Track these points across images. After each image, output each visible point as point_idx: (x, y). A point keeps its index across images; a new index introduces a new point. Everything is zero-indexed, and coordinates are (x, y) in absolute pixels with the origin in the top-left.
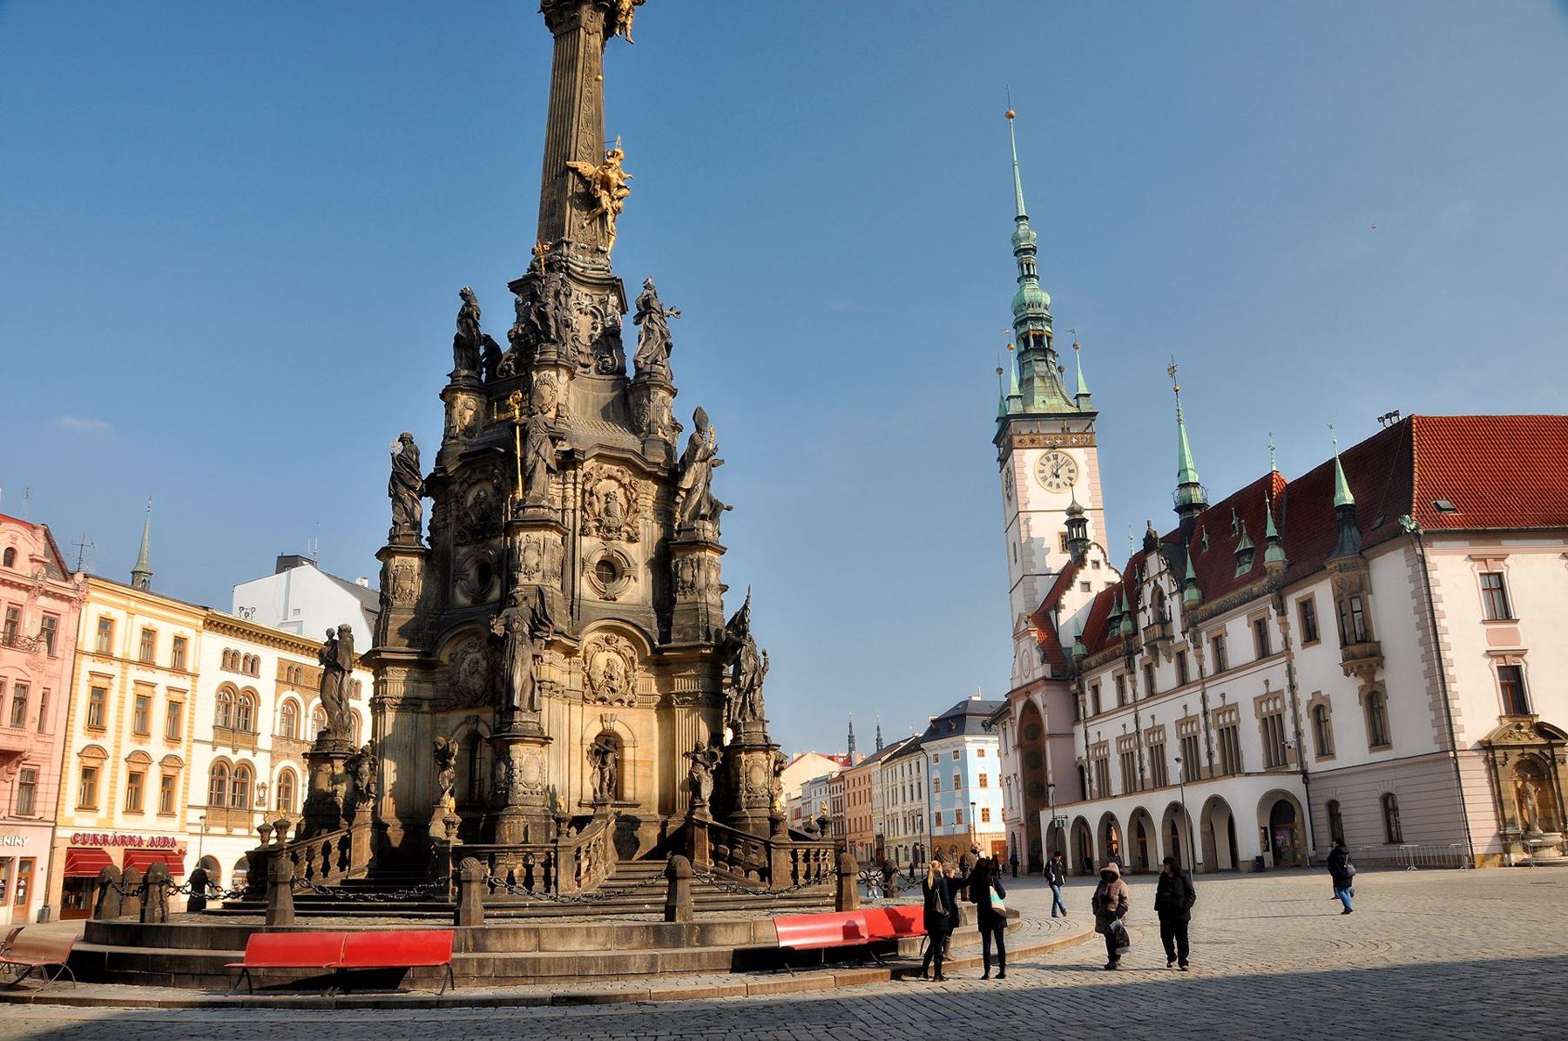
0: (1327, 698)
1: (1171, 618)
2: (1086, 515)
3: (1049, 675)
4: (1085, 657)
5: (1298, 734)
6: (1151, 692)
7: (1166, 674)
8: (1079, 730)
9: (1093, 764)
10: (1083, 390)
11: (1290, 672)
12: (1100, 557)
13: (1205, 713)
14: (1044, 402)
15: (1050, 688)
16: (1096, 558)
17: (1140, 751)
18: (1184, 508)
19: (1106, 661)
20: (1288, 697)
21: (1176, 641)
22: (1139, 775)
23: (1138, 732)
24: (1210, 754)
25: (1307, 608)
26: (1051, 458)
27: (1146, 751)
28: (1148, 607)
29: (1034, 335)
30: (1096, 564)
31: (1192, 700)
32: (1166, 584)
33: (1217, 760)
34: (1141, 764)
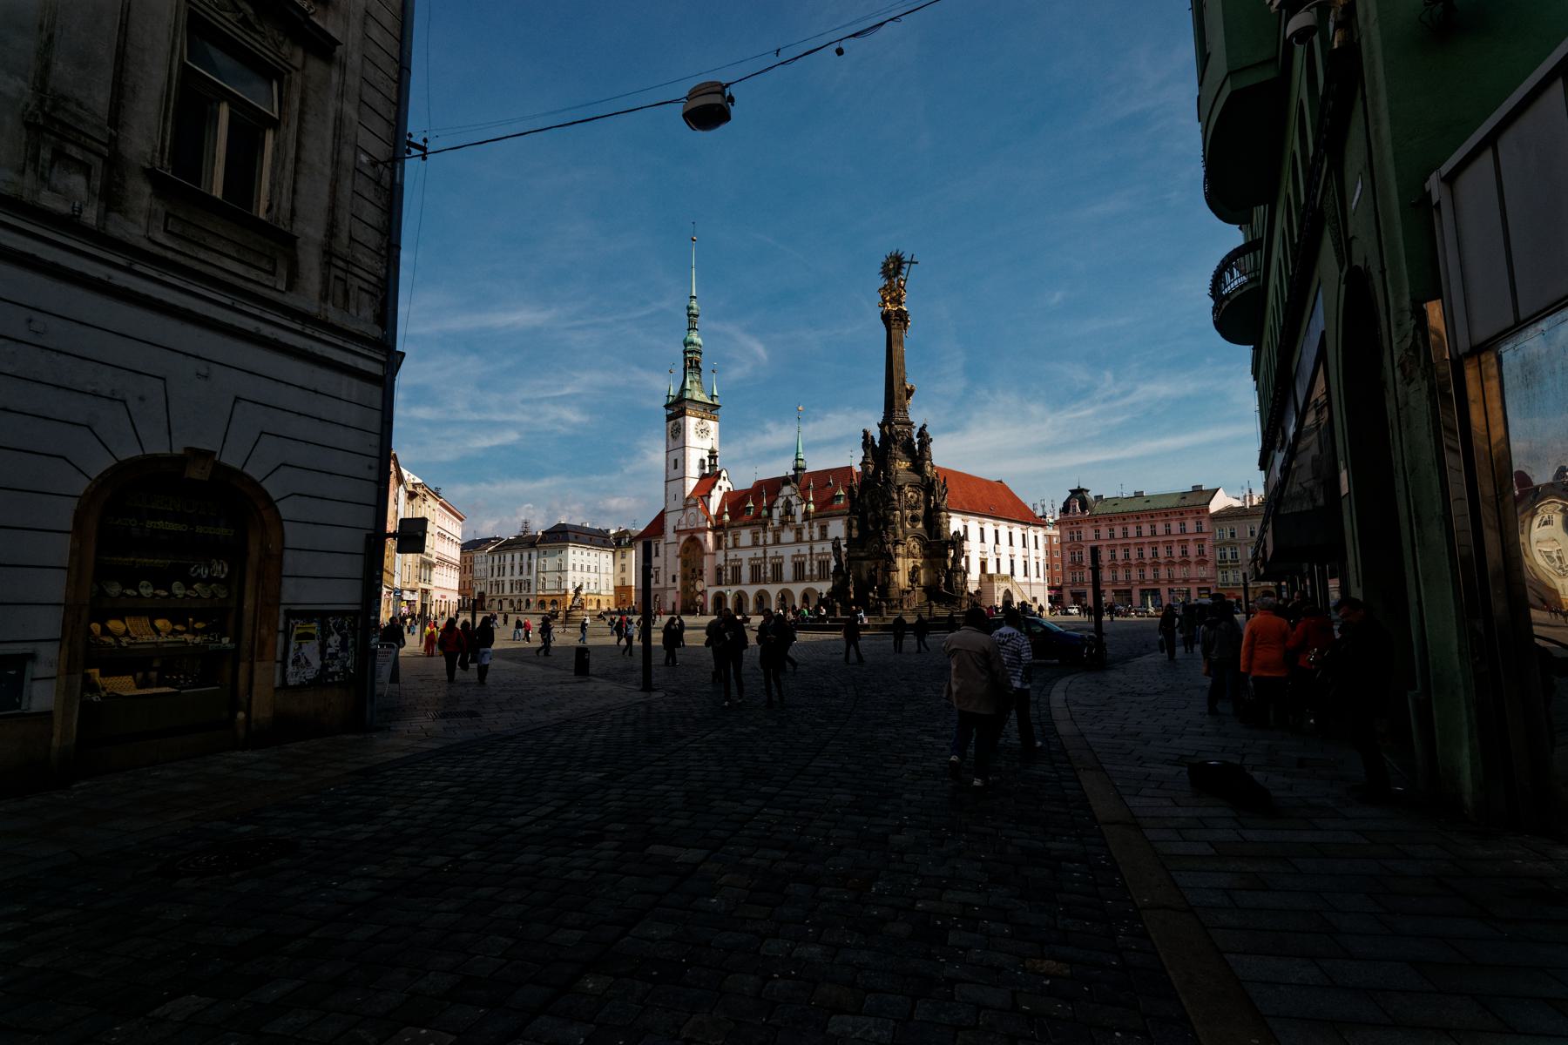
2: (717, 454)
6: (777, 541)
7: (788, 536)
8: (721, 553)
9: (729, 568)
10: (715, 393)
12: (726, 476)
13: (811, 554)
18: (796, 469)
19: (745, 526)
22: (762, 575)
23: (765, 558)
24: (812, 570)
27: (769, 566)
30: (724, 478)
31: (805, 549)
33: (815, 572)
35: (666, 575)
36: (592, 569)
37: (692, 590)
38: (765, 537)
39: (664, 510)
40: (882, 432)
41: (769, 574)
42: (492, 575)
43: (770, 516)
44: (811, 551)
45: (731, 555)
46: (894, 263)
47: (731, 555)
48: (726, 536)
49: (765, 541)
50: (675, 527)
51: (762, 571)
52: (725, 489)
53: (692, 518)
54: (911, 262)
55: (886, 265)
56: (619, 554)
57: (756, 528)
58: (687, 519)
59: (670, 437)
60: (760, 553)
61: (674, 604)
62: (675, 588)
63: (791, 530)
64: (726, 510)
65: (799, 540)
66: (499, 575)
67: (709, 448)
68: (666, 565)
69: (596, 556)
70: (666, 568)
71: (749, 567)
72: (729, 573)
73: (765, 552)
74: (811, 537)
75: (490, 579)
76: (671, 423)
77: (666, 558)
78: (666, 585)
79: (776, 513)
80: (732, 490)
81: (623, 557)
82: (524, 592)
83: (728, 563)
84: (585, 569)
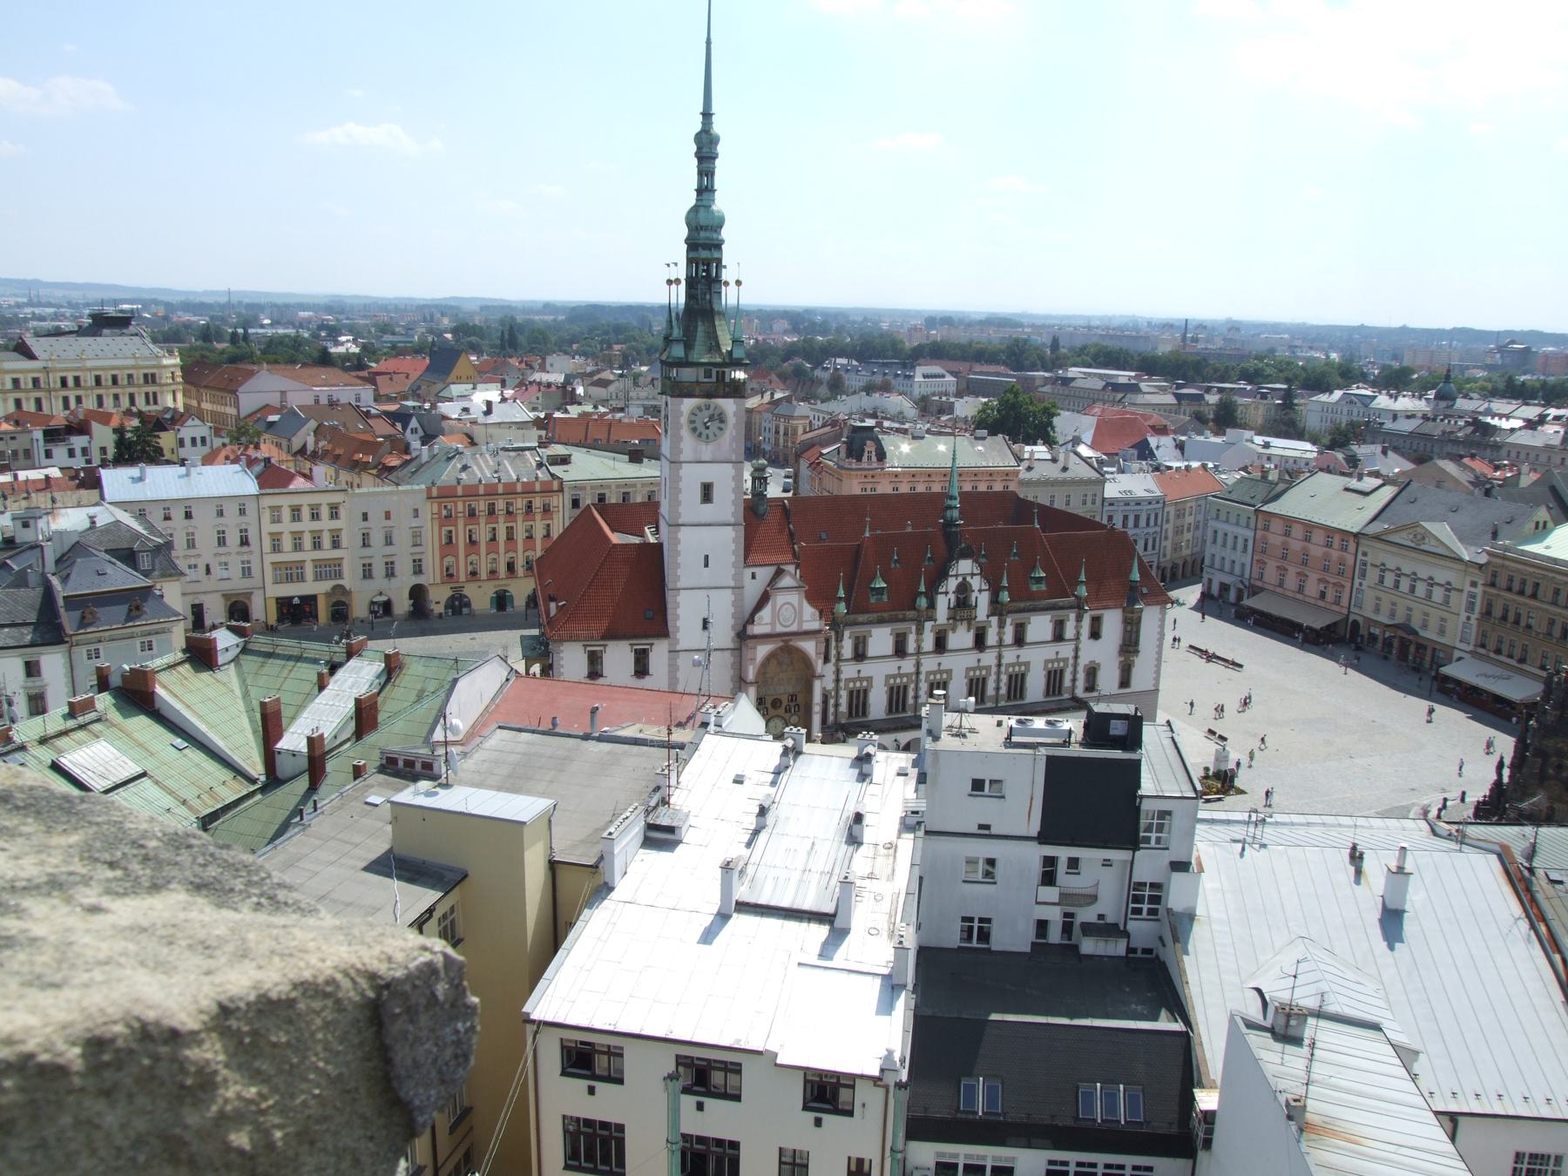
0: (1099, 665)
5: (1074, 680)
6: (940, 645)
7: (961, 638)
11: (1077, 650)
13: (999, 665)
19: (881, 622)
20: (1071, 661)
22: (910, 701)
23: (918, 673)
24: (998, 689)
25: (1096, 622)
32: (976, 583)
33: (1003, 691)
38: (919, 641)
43: (932, 605)
44: (1000, 661)
47: (849, 671)
49: (919, 647)
51: (911, 693)
53: (787, 613)
57: (901, 627)
60: (908, 665)
65: (980, 643)
72: (844, 701)
73: (918, 665)
74: (1001, 640)
79: (943, 604)
83: (842, 684)
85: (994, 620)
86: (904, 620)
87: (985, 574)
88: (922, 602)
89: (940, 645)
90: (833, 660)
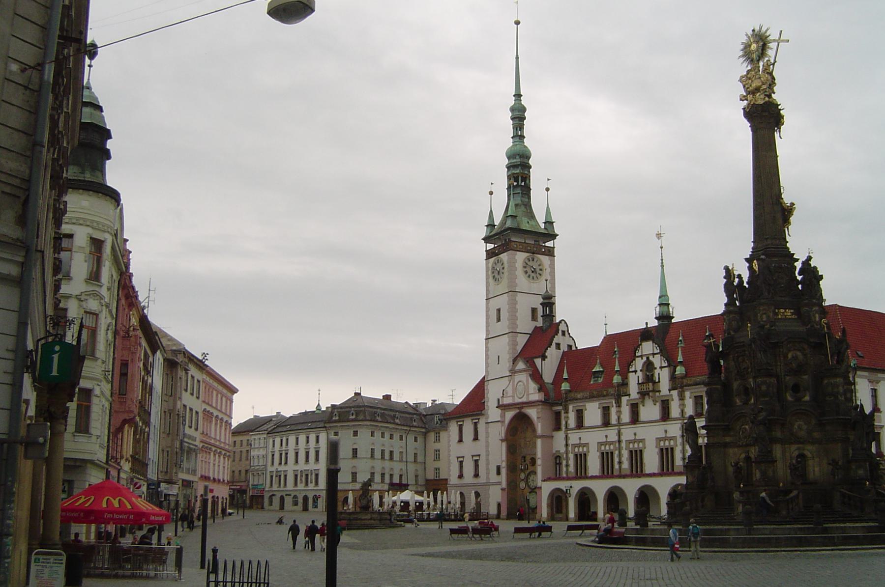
1: (659, 378)
3: (543, 400)
4: (570, 391)
6: (635, 419)
7: (650, 411)
8: (560, 436)
9: (571, 456)
14: (528, 222)
15: (543, 407)
16: (564, 330)
17: (620, 452)
19: (592, 397)
21: (662, 394)
22: (616, 466)
23: (619, 441)
26: (531, 259)
27: (625, 454)
28: (639, 371)
29: (522, 177)
30: (563, 333)
32: (657, 361)
34: (620, 459)
35: (488, 464)
36: (396, 456)
37: (522, 485)
38: (619, 413)
39: (484, 377)
40: (750, 268)
41: (626, 465)
42: (273, 463)
43: (625, 384)
45: (574, 438)
46: (757, 42)
47: (574, 438)
48: (567, 412)
50: (499, 400)
51: (616, 460)
52: (564, 348)
53: (520, 387)
54: (779, 41)
55: (747, 46)
56: (432, 436)
57: (606, 402)
58: (515, 390)
59: (491, 280)
61: (499, 505)
62: (499, 483)
63: (655, 402)
64: (565, 376)
65: (665, 416)
66: (280, 464)
67: (543, 292)
68: (487, 451)
69: (401, 438)
70: (488, 455)
71: (598, 454)
72: (572, 462)
73: (619, 434)
75: (273, 469)
76: (492, 260)
77: (487, 442)
78: (488, 478)
79: (634, 380)
80: (574, 348)
81: (437, 440)
82: (311, 486)
83: (570, 449)
84: (387, 456)
85: (675, 393)
86: (607, 395)
87: (662, 353)
88: (617, 379)
89: (635, 419)
90: (563, 428)
